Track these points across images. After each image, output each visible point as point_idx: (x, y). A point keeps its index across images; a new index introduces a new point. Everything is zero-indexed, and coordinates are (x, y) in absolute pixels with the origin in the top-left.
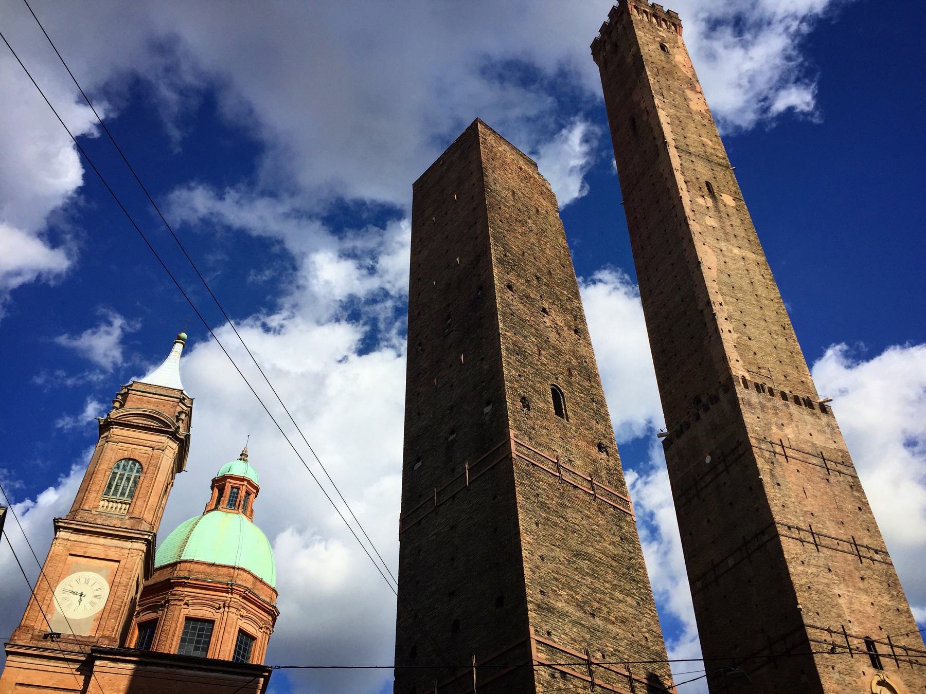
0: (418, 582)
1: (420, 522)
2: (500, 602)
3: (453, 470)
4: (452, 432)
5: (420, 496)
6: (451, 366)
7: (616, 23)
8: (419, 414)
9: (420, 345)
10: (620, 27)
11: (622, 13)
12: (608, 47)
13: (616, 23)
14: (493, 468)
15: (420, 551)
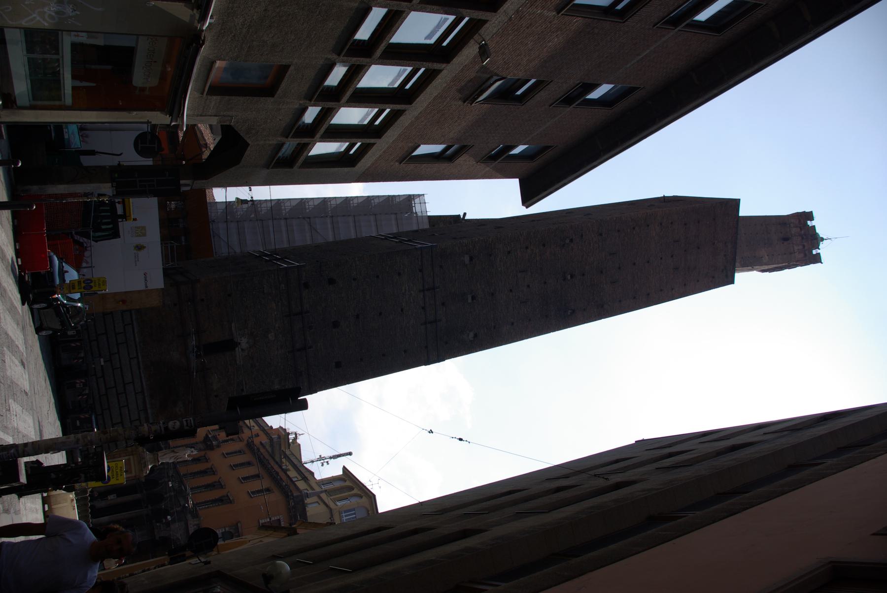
0: (378, 277)
1: (421, 271)
2: (338, 365)
3: (443, 304)
4: (473, 298)
5: (441, 267)
6: (528, 286)
7: (804, 246)
8: (509, 252)
9: (571, 240)
10: (796, 248)
11: (805, 255)
12: (794, 231)
13: (804, 246)
14: (426, 347)
15: (399, 274)
